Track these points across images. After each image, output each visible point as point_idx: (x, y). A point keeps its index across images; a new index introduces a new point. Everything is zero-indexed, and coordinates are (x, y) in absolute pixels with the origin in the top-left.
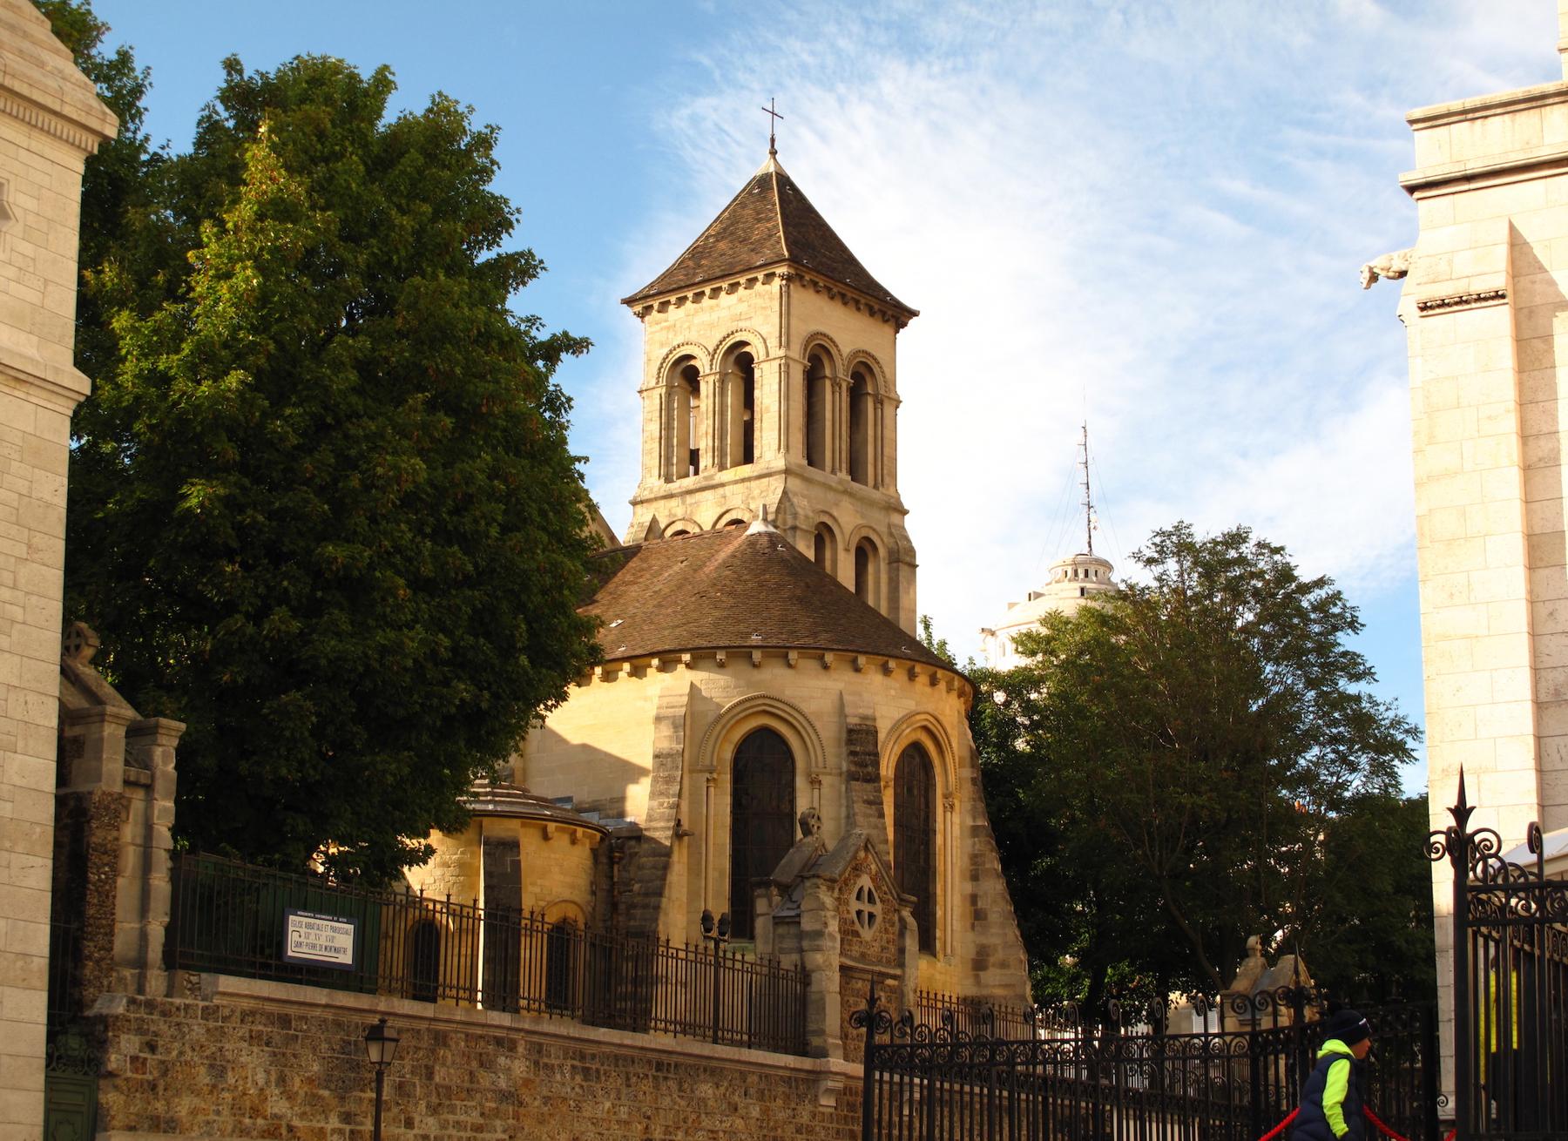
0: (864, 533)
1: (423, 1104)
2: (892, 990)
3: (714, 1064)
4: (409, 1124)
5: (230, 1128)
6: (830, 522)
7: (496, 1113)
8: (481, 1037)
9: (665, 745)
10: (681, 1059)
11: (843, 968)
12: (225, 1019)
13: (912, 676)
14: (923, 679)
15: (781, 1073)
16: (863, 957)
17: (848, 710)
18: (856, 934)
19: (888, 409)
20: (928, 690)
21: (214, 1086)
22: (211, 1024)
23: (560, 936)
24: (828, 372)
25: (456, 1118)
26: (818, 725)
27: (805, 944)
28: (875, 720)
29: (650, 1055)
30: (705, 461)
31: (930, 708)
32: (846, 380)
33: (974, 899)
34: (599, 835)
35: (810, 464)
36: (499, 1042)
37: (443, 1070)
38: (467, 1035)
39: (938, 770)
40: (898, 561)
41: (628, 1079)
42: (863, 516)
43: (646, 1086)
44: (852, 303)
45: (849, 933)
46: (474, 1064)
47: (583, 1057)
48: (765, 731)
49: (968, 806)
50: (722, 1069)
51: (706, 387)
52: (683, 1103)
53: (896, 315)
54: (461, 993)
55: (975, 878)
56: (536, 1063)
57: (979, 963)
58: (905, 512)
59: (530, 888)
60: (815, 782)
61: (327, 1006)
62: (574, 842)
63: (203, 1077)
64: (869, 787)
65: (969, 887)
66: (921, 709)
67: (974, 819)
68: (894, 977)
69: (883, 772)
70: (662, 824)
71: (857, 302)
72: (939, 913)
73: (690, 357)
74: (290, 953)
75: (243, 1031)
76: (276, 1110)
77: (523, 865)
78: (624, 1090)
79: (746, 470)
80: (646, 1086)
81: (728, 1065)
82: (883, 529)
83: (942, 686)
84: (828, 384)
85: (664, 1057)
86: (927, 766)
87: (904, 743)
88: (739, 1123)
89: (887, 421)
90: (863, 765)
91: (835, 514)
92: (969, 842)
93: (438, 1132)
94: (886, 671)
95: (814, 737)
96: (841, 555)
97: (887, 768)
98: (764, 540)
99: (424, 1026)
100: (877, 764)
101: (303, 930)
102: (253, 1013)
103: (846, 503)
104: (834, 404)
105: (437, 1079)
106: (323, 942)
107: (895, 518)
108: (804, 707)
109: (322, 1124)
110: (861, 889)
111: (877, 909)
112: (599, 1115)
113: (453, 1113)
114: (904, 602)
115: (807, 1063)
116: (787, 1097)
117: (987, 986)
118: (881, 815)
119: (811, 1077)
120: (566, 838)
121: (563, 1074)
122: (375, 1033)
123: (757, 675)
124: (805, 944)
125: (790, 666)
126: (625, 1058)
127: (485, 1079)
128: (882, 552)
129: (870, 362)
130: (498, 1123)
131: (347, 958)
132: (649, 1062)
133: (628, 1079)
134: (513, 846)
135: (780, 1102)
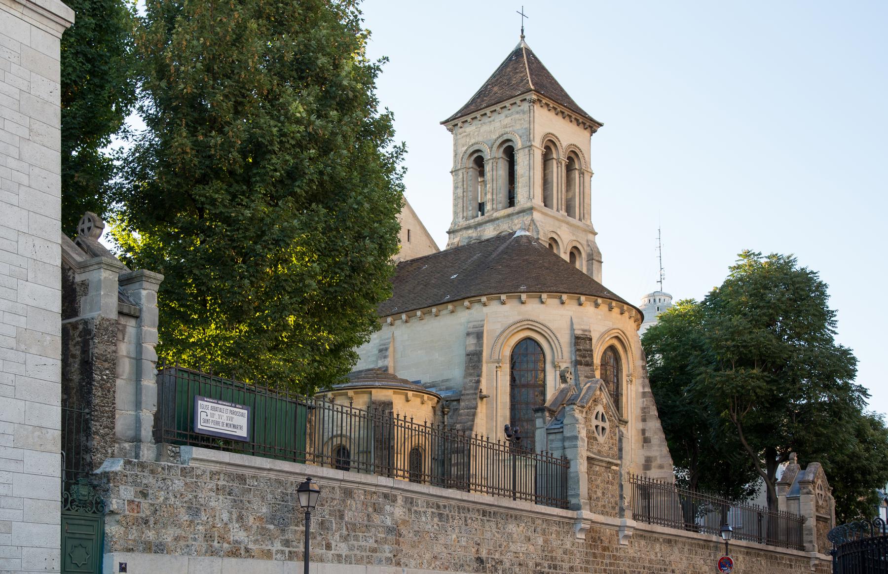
0: (575, 244)
6: (556, 237)
9: (471, 348)
13: (611, 309)
14: (616, 310)
17: (575, 327)
20: (619, 316)
24: (554, 156)
30: (488, 207)
32: (564, 161)
35: (545, 206)
42: (574, 234)
44: (567, 118)
51: (488, 168)
53: (591, 125)
70: (472, 392)
71: (570, 117)
79: (510, 210)
82: (584, 243)
83: (626, 314)
84: (555, 162)
89: (586, 184)
94: (597, 305)
98: (525, 240)
100: (591, 356)
103: (565, 227)
104: (557, 172)
107: (590, 236)
125: (542, 302)
129: (577, 151)
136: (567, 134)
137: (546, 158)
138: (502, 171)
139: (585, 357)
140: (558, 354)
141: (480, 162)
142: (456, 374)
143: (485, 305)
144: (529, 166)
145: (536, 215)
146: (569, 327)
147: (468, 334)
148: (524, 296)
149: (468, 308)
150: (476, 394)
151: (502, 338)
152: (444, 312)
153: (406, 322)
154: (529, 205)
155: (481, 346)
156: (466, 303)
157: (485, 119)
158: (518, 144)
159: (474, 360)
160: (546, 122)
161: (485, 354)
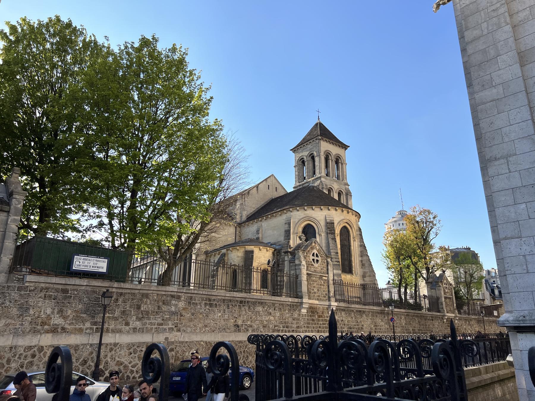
1: (134, 318)
2: (325, 280)
3: (263, 301)
4: (127, 324)
5: (28, 330)
7: (170, 319)
8: (164, 295)
9: (287, 229)
10: (249, 300)
11: (307, 274)
12: (30, 291)
13: (343, 211)
14: (345, 212)
16: (315, 271)
18: (313, 265)
19: (344, 165)
21: (21, 315)
22: (22, 293)
23: (264, 273)
25: (150, 321)
29: (237, 299)
30: (306, 178)
31: (348, 218)
32: (334, 160)
33: (362, 261)
36: (173, 296)
37: (145, 306)
38: (158, 294)
39: (351, 232)
41: (228, 306)
43: (237, 308)
45: (309, 265)
46: (161, 303)
47: (210, 300)
48: (309, 225)
49: (359, 240)
50: (265, 303)
51: (306, 164)
52: (250, 313)
53: (345, 147)
54: (176, 283)
55: (362, 256)
56: (189, 303)
57: (364, 276)
60: (320, 235)
61: (87, 286)
62: (267, 251)
63: (15, 311)
65: (360, 259)
68: (325, 277)
69: (336, 232)
72: (353, 265)
73: (303, 158)
74: (74, 268)
75: (42, 294)
76: (56, 322)
77: (254, 256)
78: (227, 310)
80: (237, 308)
81: (267, 301)
82: (344, 189)
83: (350, 213)
85: (243, 299)
86: (348, 231)
87: (342, 226)
88: (272, 318)
90: (331, 231)
93: (141, 327)
94: (336, 210)
96: (335, 194)
97: (337, 231)
99: (137, 291)
100: (334, 230)
101: (81, 261)
102: (47, 288)
103: (335, 183)
105: (142, 309)
106: (92, 264)
107: (347, 187)
108: (317, 219)
109: (82, 326)
111: (319, 259)
112: (216, 318)
113: (149, 320)
114: (349, 203)
115: (296, 300)
116: (290, 310)
118: (336, 242)
119: (299, 304)
121: (201, 306)
122: (104, 295)
123: (306, 212)
126: (227, 300)
127: (164, 308)
128: (344, 193)
130: (170, 322)
131: (104, 270)
132: (237, 301)
133: (228, 306)
134: (252, 252)
136: (334, 150)
137: (327, 160)
138: (311, 165)
141: (303, 162)
142: (282, 239)
143: (291, 212)
144: (320, 162)
145: (323, 179)
148: (306, 208)
151: (298, 224)
154: (320, 176)
155: (290, 227)
156: (285, 211)
157: (305, 147)
158: (315, 153)
159: (287, 233)
160: (325, 146)
161: (291, 231)
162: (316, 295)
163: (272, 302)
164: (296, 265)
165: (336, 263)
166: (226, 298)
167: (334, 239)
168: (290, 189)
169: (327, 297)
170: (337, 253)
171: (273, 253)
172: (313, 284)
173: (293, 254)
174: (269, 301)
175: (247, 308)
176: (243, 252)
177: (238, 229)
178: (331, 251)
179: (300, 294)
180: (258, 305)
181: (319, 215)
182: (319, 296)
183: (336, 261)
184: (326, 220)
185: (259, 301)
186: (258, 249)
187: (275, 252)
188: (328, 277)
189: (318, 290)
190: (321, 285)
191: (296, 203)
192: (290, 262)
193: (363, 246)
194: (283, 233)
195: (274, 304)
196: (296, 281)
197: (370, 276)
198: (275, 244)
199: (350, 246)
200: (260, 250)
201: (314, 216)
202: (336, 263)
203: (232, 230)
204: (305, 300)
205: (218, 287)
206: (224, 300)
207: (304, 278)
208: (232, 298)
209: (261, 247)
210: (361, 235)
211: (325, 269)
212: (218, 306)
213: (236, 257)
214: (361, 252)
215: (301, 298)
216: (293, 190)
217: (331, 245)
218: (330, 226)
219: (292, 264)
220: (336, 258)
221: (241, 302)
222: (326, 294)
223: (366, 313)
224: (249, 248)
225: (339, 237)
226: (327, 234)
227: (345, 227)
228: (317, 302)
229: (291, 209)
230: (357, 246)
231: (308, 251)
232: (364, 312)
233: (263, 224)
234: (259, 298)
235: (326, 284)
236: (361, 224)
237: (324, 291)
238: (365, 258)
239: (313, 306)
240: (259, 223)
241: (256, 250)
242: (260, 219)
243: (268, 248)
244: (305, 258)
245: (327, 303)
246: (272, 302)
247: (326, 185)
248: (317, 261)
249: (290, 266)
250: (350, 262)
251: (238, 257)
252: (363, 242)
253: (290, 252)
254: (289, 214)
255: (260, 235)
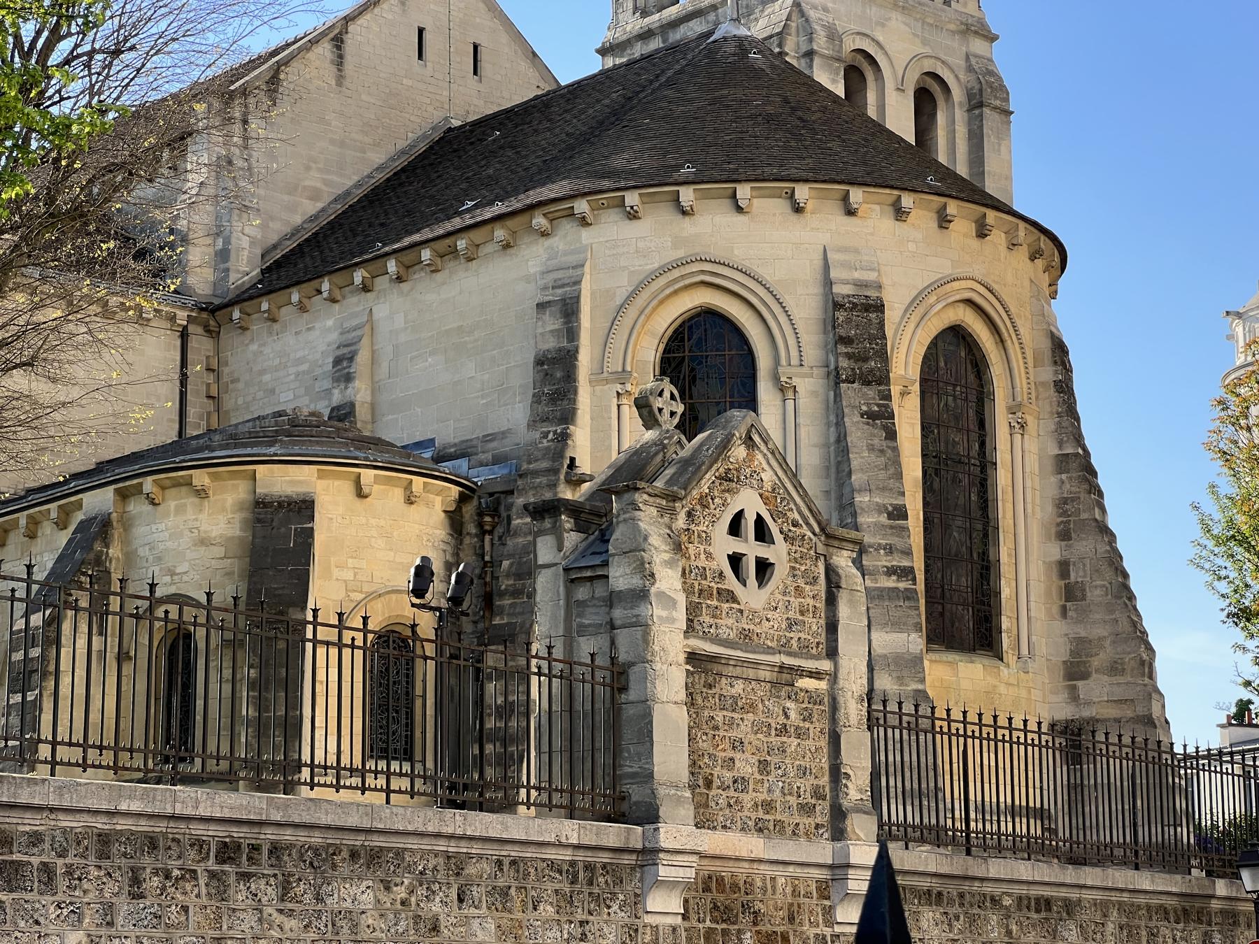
0: (928, 66)
3: (378, 841)
9: (550, 344)
10: (287, 835)
11: (692, 657)
13: (944, 221)
14: (962, 227)
15: (551, 854)
18: (731, 597)
20: (975, 243)
26: (789, 301)
27: (618, 613)
28: (879, 287)
31: (978, 271)
33: (1063, 568)
34: (455, 491)
40: (981, 105)
41: (136, 881)
42: (925, 42)
43: (196, 895)
45: (702, 599)
50: (399, 853)
55: (1064, 535)
57: (1075, 671)
58: (992, 38)
59: (336, 573)
60: (784, 389)
62: (409, 501)
64: (871, 392)
65: (1055, 551)
66: (959, 272)
67: (1061, 444)
70: (544, 465)
72: (1006, 592)
78: (124, 906)
80: (196, 895)
81: (412, 843)
83: (998, 237)
86: (979, 364)
91: (881, 39)
92: (1054, 479)
94: (900, 213)
95: (782, 319)
96: (892, 97)
97: (906, 363)
98: (730, 48)
100: (883, 356)
103: (897, 21)
110: (739, 516)
111: (777, 553)
114: (991, 165)
115: (612, 834)
116: (566, 901)
117: (1089, 703)
118: (891, 435)
120: (398, 494)
123: (687, 227)
124: (618, 613)
125: (739, 209)
126: (131, 836)
128: (957, 94)
132: (199, 844)
133: (136, 881)
134: (304, 508)
135: (547, 910)
139: (866, 360)
140: (789, 350)
142: (513, 416)
143: (584, 222)
146: (819, 277)
147: (541, 306)
148: (687, 195)
149: (544, 234)
150: (556, 471)
151: (632, 312)
152: (489, 248)
153: (399, 279)
155: (572, 333)
156: (539, 220)
159: (555, 379)
162: (747, 799)
163: (441, 846)
164: (612, 599)
165: (891, 582)
166: (122, 824)
167: (882, 417)
168: (573, 62)
169: (823, 808)
170: (899, 513)
171: (454, 519)
172: (731, 724)
173: (595, 520)
174: (425, 844)
175: (269, 892)
176: (241, 507)
177: (200, 344)
178: (861, 499)
179: (636, 793)
180: (344, 869)
181: (779, 249)
182: (768, 806)
183: (891, 571)
184: (828, 283)
185: (358, 841)
186: (347, 487)
187: (469, 510)
188: (834, 677)
189: (763, 766)
190: (783, 730)
191: (618, 162)
192: (573, 576)
193: (1076, 466)
194: (520, 376)
195: (456, 864)
196: (615, 710)
197: (1115, 669)
198: (463, 452)
199: (986, 465)
200: (361, 494)
201: (739, 255)
202: (891, 582)
203: (155, 351)
204: (676, 831)
205: (63, 753)
206: (104, 840)
207: (668, 683)
208: (161, 827)
209: (368, 475)
210: (1064, 387)
211: (816, 625)
212: (62, 883)
213: (186, 542)
214: (1063, 504)
215: (649, 816)
216: (593, 65)
217: (860, 458)
218: (855, 327)
219: (582, 593)
220: (890, 550)
221: (228, 852)
222: (817, 794)
223: (1084, 916)
224: (281, 480)
225: (914, 401)
226: (835, 379)
227: (957, 333)
228: (753, 845)
229: (582, 206)
230: (1033, 463)
231: (703, 502)
232: (1070, 907)
233: (381, 311)
234: (353, 821)
235: (819, 725)
236: (1071, 313)
237: (803, 772)
238: (1085, 546)
239: (725, 870)
240: (355, 305)
241: (330, 493)
242: (359, 276)
243: (418, 482)
244: (678, 548)
245: (823, 851)
246: (441, 846)
247: (834, 36)
248: (764, 568)
249: (572, 607)
250: (985, 571)
251: (204, 542)
252: (1079, 439)
253: (574, 510)
254: (566, 238)
255: (360, 392)
